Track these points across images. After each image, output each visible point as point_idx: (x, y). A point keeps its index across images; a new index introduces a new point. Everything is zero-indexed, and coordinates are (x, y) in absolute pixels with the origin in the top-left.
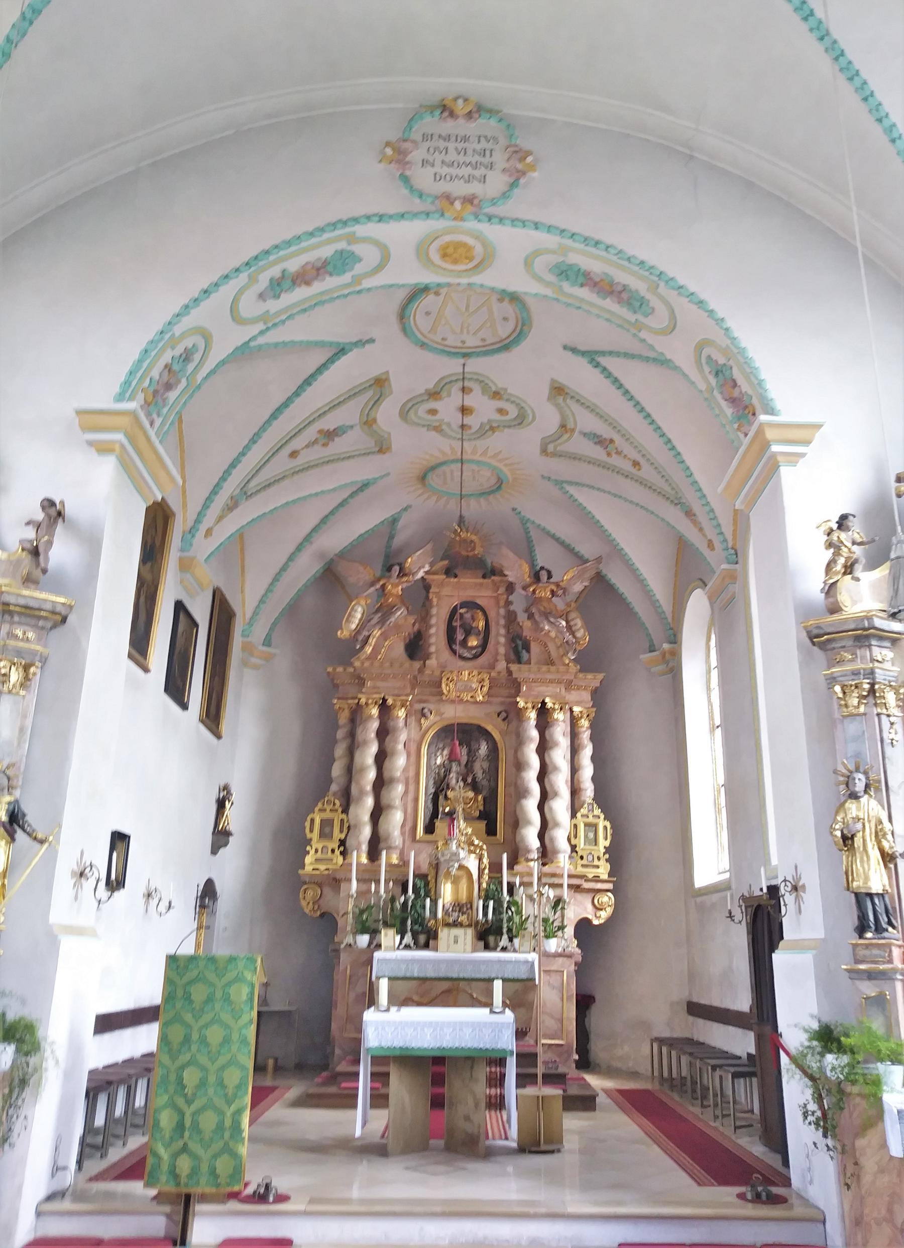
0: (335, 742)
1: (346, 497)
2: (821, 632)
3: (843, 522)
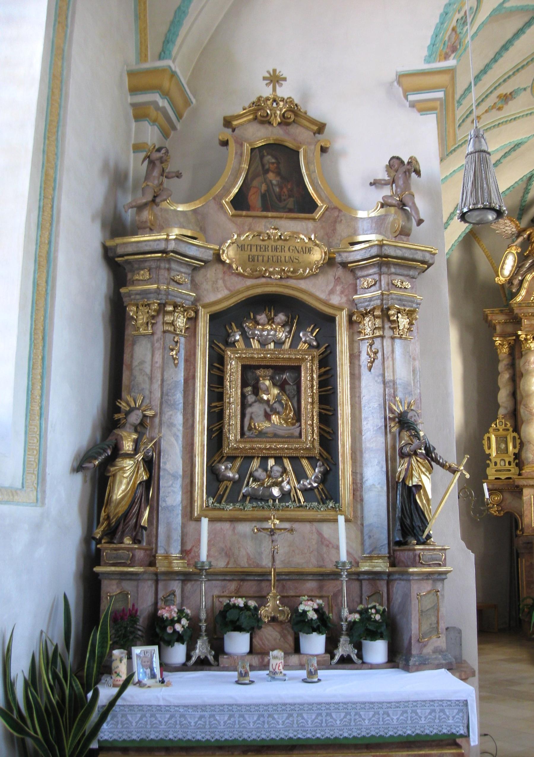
0: (496, 373)
1: (498, 158)
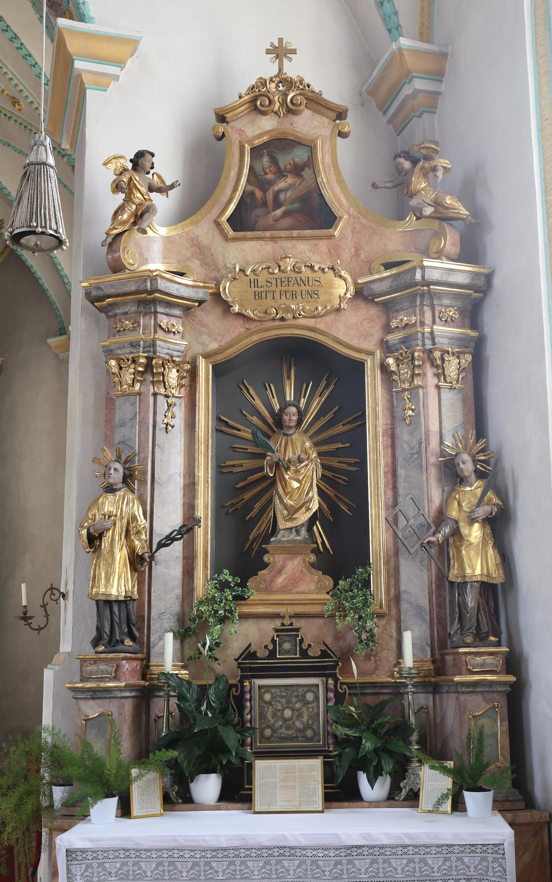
2: (101, 293)
3: (140, 161)
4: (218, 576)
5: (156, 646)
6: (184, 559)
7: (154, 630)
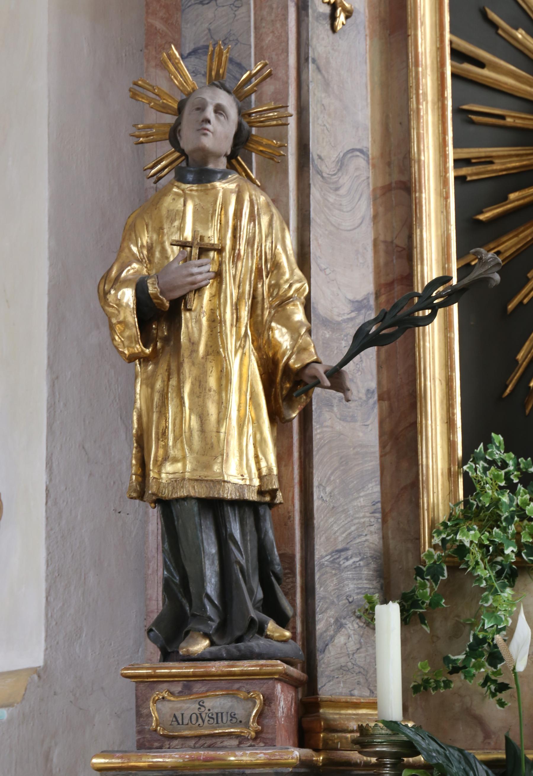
4: (486, 449)
5: (330, 647)
6: (381, 398)
7: (324, 598)
